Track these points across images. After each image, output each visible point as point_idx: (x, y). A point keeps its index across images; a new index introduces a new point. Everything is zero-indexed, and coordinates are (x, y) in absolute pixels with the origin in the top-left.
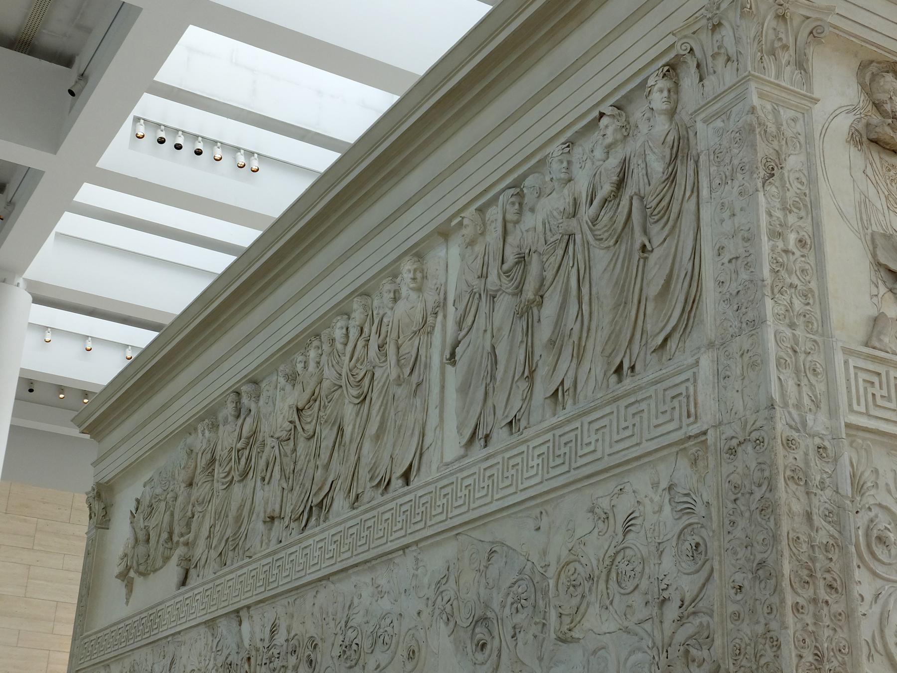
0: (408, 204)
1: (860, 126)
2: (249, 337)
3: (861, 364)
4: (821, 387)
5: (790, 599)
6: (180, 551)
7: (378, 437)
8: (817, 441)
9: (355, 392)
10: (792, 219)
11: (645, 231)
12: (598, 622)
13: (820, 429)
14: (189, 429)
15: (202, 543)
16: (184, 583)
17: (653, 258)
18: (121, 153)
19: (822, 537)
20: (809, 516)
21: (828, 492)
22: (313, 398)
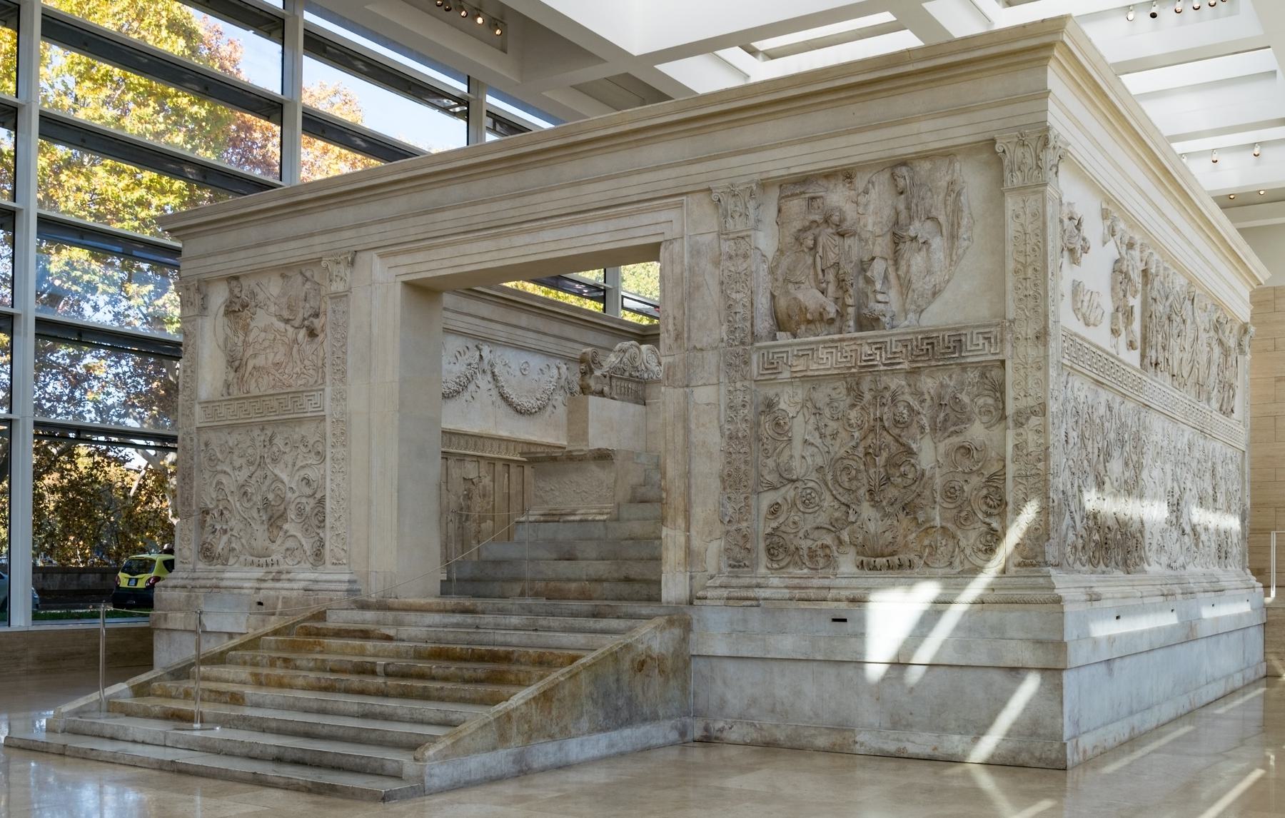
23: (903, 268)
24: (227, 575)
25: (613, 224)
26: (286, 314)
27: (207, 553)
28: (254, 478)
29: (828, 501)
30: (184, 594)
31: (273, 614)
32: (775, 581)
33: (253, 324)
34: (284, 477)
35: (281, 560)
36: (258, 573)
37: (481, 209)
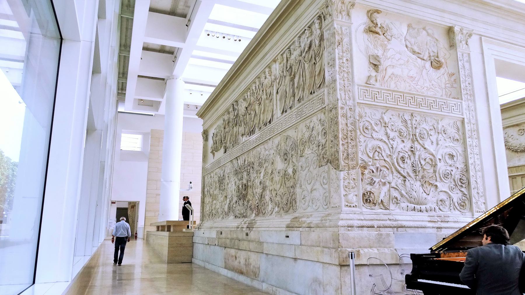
0: (266, 54)
1: (367, 28)
2: (234, 91)
3: (362, 88)
4: (351, 94)
5: (341, 142)
6: (224, 144)
7: (263, 113)
8: (350, 107)
9: (258, 102)
10: (344, 54)
11: (315, 59)
12: (307, 152)
13: (351, 104)
14: (223, 115)
15: (228, 142)
17: (317, 65)
18: (203, 40)
19: (350, 129)
20: (347, 124)
21: (352, 118)
22: (249, 105)
27: (368, 199)
30: (373, 233)
33: (389, 46)
35: (437, 208)
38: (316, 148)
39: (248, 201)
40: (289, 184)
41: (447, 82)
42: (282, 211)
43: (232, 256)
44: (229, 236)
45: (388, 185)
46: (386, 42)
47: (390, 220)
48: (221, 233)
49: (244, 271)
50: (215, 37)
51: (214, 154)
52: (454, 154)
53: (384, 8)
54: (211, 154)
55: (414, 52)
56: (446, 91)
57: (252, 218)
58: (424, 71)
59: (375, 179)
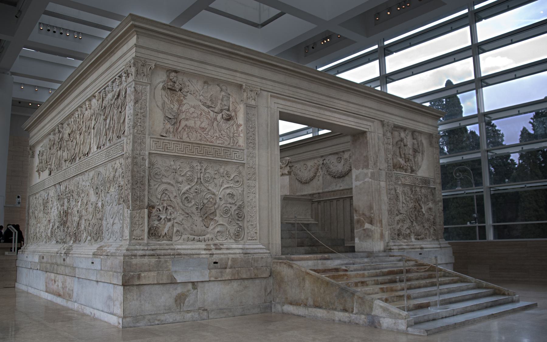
0: (87, 88)
2: (59, 113)
3: (155, 140)
6: (49, 166)
7: (83, 144)
11: (121, 108)
12: (112, 189)
15: (53, 164)
16: (50, 175)
18: (36, 36)
22: (72, 132)
23: (416, 160)
24: (179, 247)
25: (356, 120)
26: (209, 103)
28: (192, 190)
29: (409, 221)
30: (153, 260)
31: (226, 268)
32: (404, 244)
33: (185, 101)
34: (214, 190)
35: (214, 238)
36: (202, 245)
37: (316, 95)
38: (117, 188)
39: (68, 228)
40: (99, 216)
41: (236, 132)
42: (93, 240)
43: (52, 280)
44: (50, 261)
45: (172, 222)
46: (182, 98)
47: (171, 249)
48: (43, 258)
49: (62, 293)
50: (51, 31)
51: (39, 174)
52: (234, 193)
53: (181, 69)
54: (37, 173)
55: (209, 107)
56: (233, 140)
57: (70, 244)
58: (215, 123)
59: (161, 216)
